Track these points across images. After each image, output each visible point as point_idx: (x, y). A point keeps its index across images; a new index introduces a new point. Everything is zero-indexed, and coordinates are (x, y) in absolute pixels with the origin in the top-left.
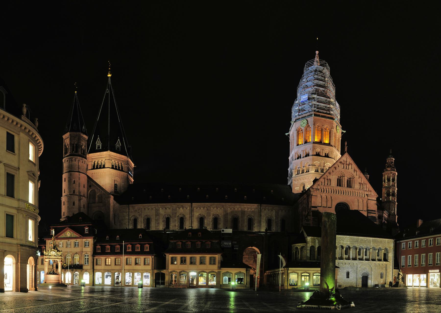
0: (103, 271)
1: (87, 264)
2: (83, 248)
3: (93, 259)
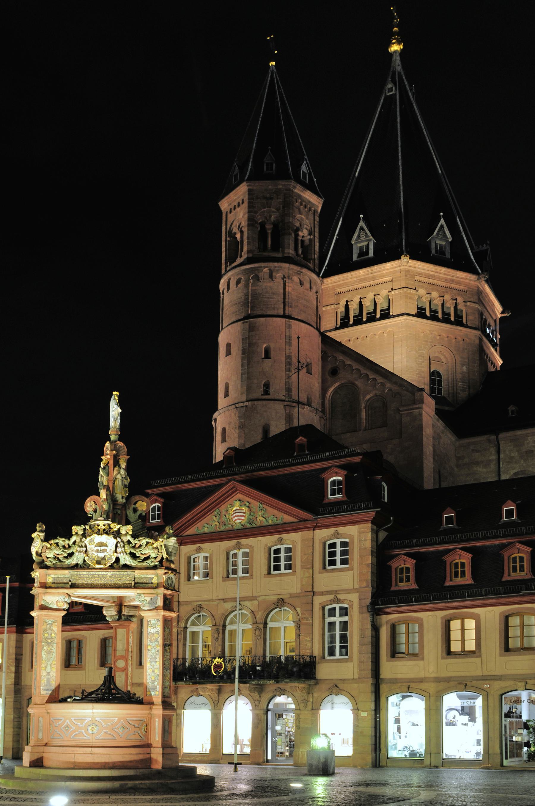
0: (432, 687)
1: (337, 656)
2: (317, 576)
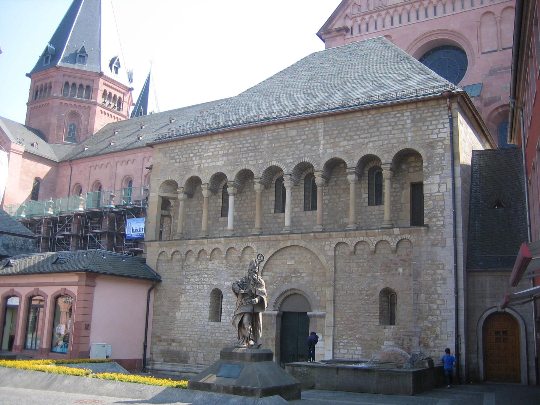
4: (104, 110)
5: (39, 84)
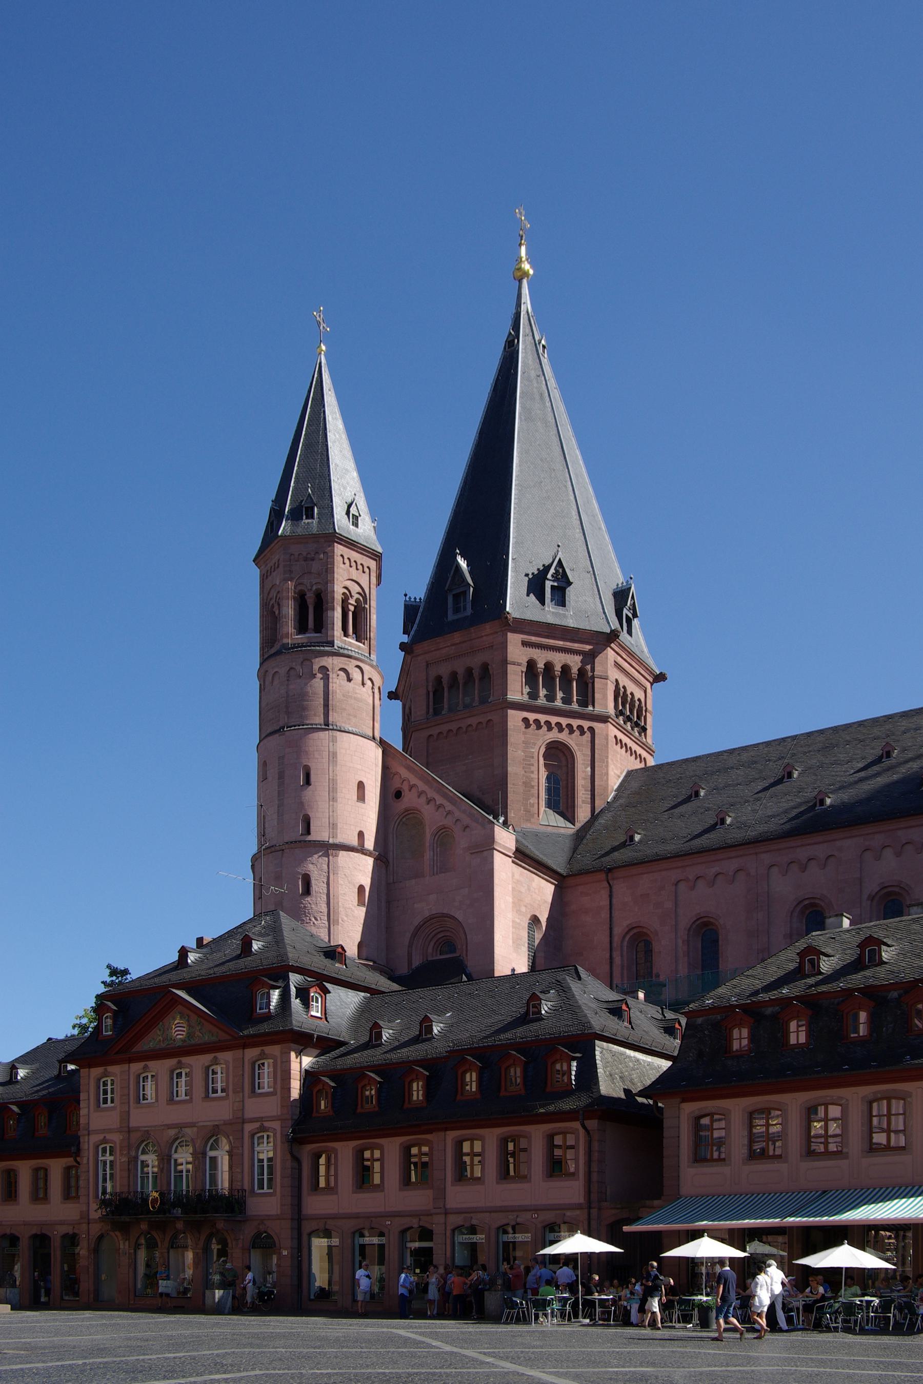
3: (297, 1160)
4: (620, 736)
5: (444, 670)
